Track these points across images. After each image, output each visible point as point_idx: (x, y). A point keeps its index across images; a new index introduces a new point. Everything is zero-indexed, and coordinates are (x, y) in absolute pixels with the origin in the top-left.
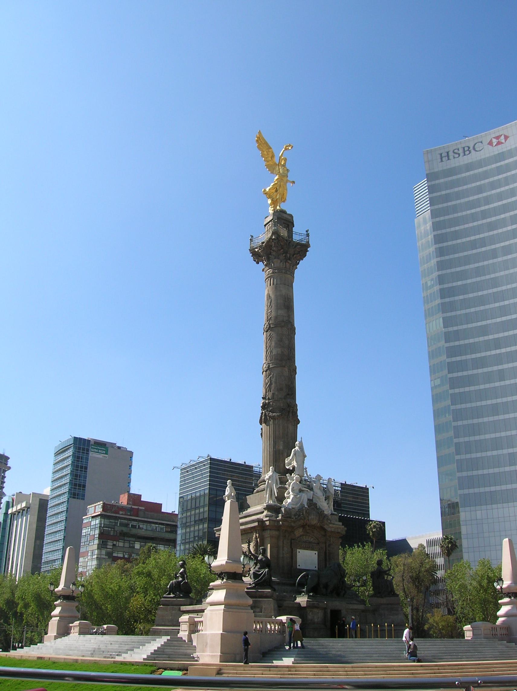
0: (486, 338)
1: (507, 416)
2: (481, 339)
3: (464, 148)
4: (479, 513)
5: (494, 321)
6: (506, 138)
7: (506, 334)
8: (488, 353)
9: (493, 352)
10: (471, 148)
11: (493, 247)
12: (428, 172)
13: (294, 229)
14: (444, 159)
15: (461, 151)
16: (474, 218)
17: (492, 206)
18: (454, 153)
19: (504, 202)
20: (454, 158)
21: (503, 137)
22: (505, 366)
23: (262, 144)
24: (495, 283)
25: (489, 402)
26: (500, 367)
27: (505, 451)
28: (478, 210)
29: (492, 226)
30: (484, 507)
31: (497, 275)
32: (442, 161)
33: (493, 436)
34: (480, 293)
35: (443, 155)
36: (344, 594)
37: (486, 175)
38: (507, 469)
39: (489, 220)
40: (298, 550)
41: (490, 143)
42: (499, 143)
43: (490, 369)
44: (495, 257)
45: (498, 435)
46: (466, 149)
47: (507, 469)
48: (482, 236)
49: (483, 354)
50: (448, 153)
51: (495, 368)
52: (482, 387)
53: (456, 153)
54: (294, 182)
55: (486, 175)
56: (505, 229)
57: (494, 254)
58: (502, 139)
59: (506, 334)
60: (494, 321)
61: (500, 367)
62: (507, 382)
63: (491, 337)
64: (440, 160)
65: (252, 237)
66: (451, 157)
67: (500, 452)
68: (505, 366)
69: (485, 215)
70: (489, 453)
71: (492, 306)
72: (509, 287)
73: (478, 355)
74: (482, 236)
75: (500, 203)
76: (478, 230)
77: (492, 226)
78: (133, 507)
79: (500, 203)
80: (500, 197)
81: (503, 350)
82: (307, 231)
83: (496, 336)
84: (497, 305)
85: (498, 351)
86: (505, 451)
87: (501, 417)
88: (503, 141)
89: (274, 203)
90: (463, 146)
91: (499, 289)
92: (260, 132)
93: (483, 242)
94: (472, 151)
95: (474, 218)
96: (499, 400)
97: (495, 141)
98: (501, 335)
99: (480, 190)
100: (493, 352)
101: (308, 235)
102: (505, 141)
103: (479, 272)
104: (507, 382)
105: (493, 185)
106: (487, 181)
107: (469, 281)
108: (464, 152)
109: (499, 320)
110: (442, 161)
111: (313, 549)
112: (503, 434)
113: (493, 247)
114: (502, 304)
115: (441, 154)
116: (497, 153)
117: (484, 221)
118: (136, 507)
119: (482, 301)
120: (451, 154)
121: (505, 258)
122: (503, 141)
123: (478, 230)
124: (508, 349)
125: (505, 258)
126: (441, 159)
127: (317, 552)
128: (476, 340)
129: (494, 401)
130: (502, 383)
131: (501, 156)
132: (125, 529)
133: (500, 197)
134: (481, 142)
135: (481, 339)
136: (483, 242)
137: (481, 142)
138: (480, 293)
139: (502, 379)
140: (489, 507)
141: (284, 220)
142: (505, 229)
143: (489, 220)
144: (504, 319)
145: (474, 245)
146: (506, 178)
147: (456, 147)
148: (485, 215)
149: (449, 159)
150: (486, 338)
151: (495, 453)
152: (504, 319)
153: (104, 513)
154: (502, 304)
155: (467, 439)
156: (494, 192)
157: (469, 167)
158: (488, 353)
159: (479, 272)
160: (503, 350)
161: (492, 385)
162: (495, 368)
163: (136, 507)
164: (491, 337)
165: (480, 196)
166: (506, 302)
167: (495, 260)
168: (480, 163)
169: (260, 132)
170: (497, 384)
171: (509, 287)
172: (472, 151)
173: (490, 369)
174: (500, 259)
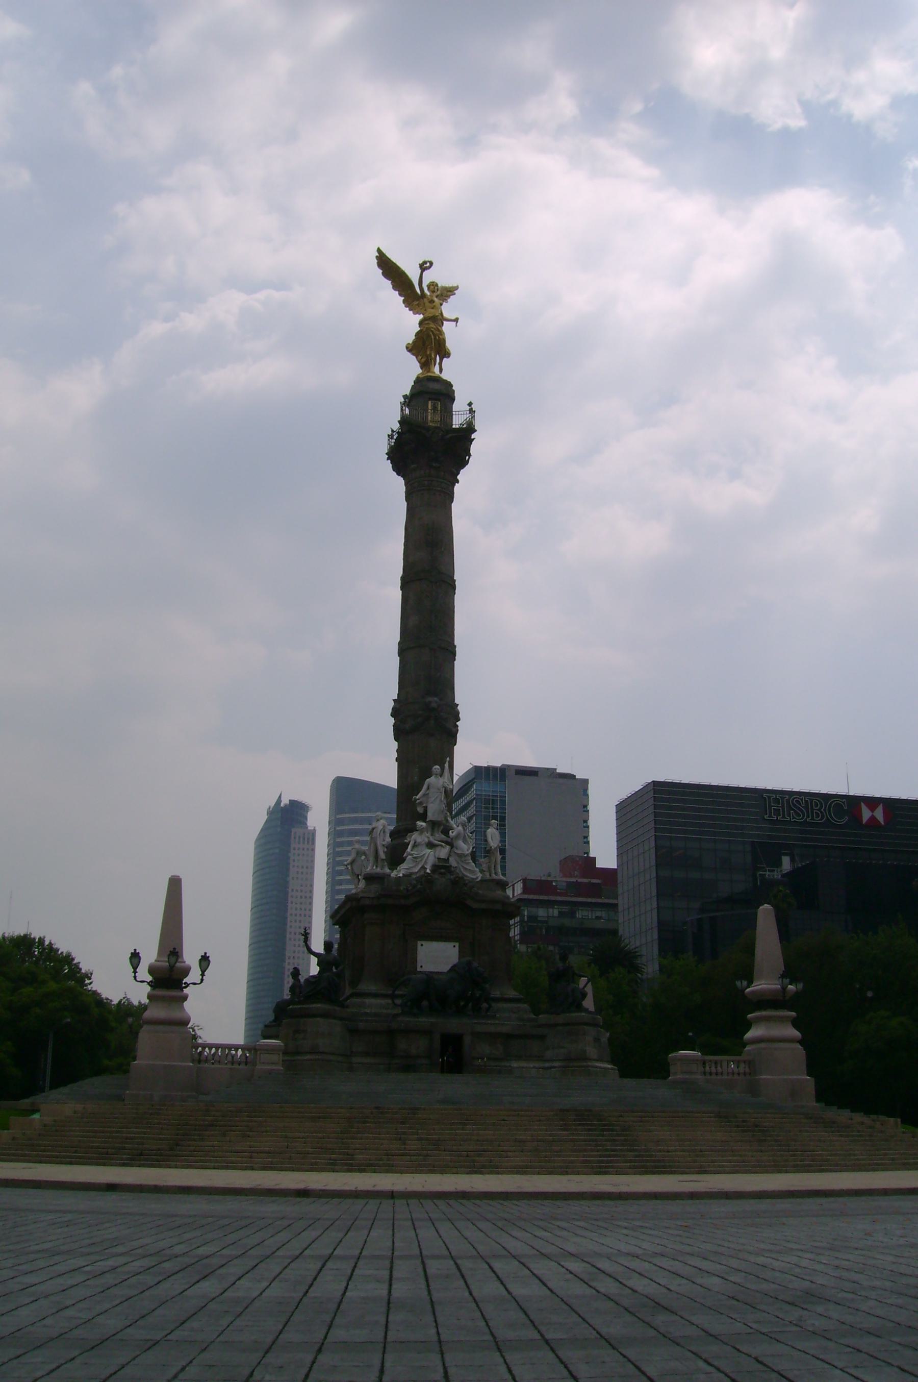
13: (456, 406)
23: (387, 267)
36: (487, 1010)
40: (419, 943)
54: (456, 320)
65: (393, 431)
78: (580, 880)
82: (470, 404)
89: (426, 364)
92: (379, 250)
101: (472, 411)
118: (585, 880)
127: (457, 944)
132: (567, 922)
141: (431, 394)
153: (526, 896)
163: (585, 880)
169: (379, 250)
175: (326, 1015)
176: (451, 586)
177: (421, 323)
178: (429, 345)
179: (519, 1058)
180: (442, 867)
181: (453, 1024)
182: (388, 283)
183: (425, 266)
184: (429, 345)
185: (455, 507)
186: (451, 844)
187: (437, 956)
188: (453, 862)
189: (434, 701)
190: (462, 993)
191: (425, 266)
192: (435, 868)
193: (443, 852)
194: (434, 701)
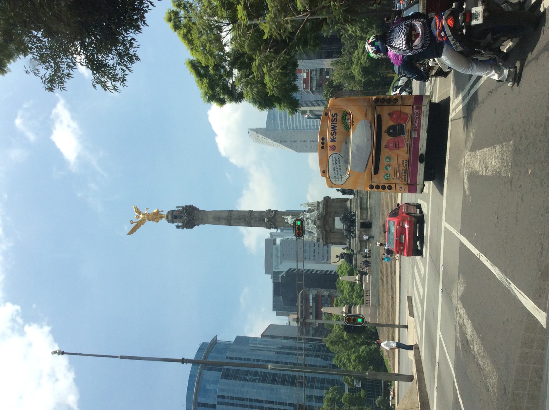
89: (162, 218)
111: (334, 220)
175: (356, 260)
176: (231, 211)
177: (149, 220)
178: (156, 217)
179: (367, 205)
180: (314, 222)
181: (357, 224)
182: (138, 230)
183: (132, 222)
184: (156, 217)
185: (207, 209)
186: (307, 219)
187: (338, 224)
188: (312, 219)
189: (266, 220)
190: (349, 219)
191: (132, 222)
192: (315, 224)
193: (310, 221)
194: (266, 220)
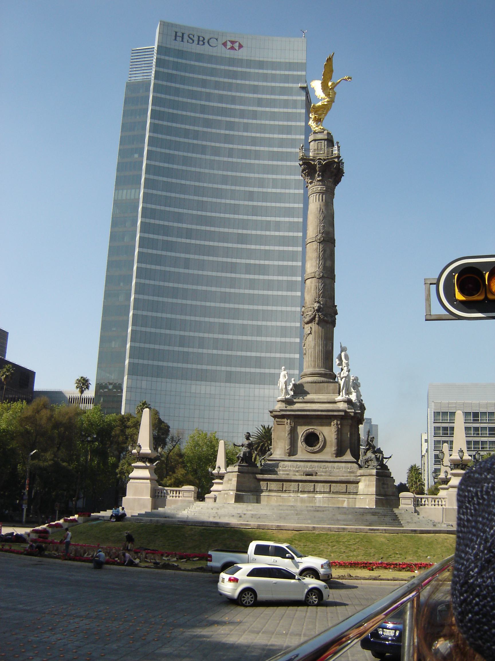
0: (180, 225)
1: (184, 302)
2: (176, 225)
3: (199, 37)
4: (144, 383)
5: (190, 212)
6: (240, 46)
7: (199, 227)
8: (179, 240)
9: (184, 240)
10: (206, 41)
11: (204, 143)
12: (160, 45)
14: (178, 38)
15: (196, 39)
16: (193, 108)
17: (211, 104)
18: (189, 37)
19: (224, 105)
20: (188, 42)
21: (237, 44)
22: (192, 256)
24: (199, 177)
25: (171, 285)
26: (187, 256)
27: (177, 333)
28: (198, 102)
29: (208, 123)
30: (149, 378)
31: (202, 170)
32: (175, 39)
33: (169, 316)
34: (183, 182)
35: (179, 34)
37: (213, 72)
38: (176, 349)
39: (206, 116)
41: (225, 44)
42: (232, 48)
43: (178, 255)
44: (203, 153)
45: (173, 316)
46: (201, 39)
47: (176, 349)
48: (196, 128)
49: (174, 239)
50: (183, 34)
51: (183, 255)
52: (168, 269)
53: (191, 39)
55: (213, 72)
56: (218, 131)
57: (203, 150)
58: (236, 46)
59: (199, 227)
60: (190, 212)
61: (187, 256)
62: (191, 271)
63: (185, 226)
64: (174, 38)
66: (185, 40)
67: (172, 332)
68: (192, 256)
69: (203, 109)
70: (163, 331)
71: (191, 197)
72: (210, 185)
73: (170, 239)
74: (196, 128)
75: (220, 105)
76: (194, 121)
77: (208, 123)
79: (220, 105)
80: (221, 99)
81: (193, 242)
83: (189, 226)
84: (196, 198)
85: (188, 241)
86: (177, 333)
87: (179, 301)
88: (237, 48)
90: (200, 34)
91: (201, 184)
93: (196, 135)
94: (206, 44)
95: (193, 108)
96: (180, 286)
97: (229, 45)
98: (194, 227)
99: (204, 83)
100: (184, 240)
102: (239, 49)
103: (186, 161)
104: (191, 271)
105: (217, 85)
106: (213, 78)
107: (175, 167)
108: (199, 40)
109: (195, 212)
110: (175, 39)
112: (178, 317)
113: (204, 143)
114: (200, 199)
115: (176, 33)
116: (228, 56)
117: (202, 116)
119: (184, 189)
120: (186, 37)
121: (212, 158)
122: (237, 48)
123: (194, 121)
124: (198, 242)
125: (212, 158)
126: (176, 36)
128: (171, 224)
129: (176, 285)
130: (186, 271)
131: (232, 62)
133: (221, 99)
134: (217, 40)
135: (176, 225)
136: (196, 135)
137: (217, 40)
138: (183, 182)
139: (187, 267)
140: (154, 379)
142: (218, 131)
143: (206, 116)
144: (199, 213)
145: (186, 134)
146: (231, 84)
147: (191, 32)
148: (203, 109)
149: (182, 41)
150: (180, 225)
151: (168, 332)
152: (199, 213)
154: (200, 199)
155: (145, 313)
156: (216, 92)
157: (199, 57)
158: (179, 240)
159: (186, 161)
160: (193, 242)
161: (177, 270)
162: (183, 255)
164: (185, 226)
165: (203, 90)
166: (205, 199)
167: (203, 156)
168: (211, 59)
170: (182, 270)
171: (210, 185)
172: (206, 44)
173: (178, 255)
174: (208, 157)
